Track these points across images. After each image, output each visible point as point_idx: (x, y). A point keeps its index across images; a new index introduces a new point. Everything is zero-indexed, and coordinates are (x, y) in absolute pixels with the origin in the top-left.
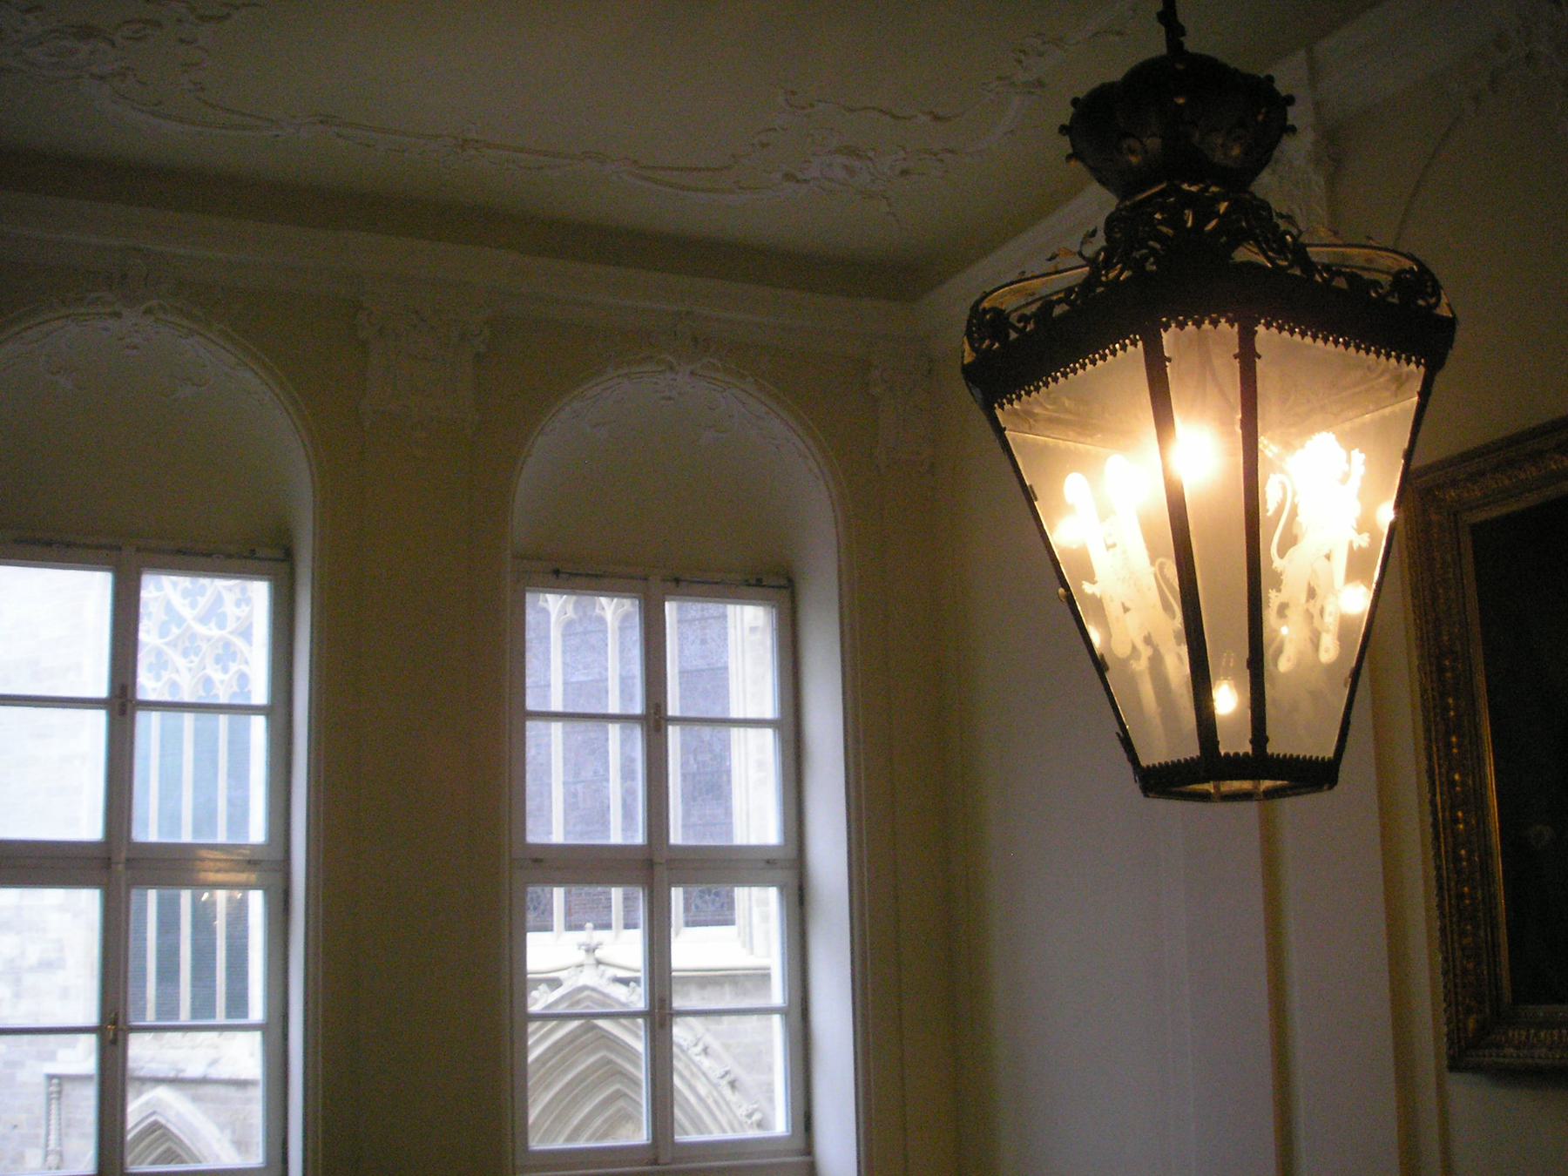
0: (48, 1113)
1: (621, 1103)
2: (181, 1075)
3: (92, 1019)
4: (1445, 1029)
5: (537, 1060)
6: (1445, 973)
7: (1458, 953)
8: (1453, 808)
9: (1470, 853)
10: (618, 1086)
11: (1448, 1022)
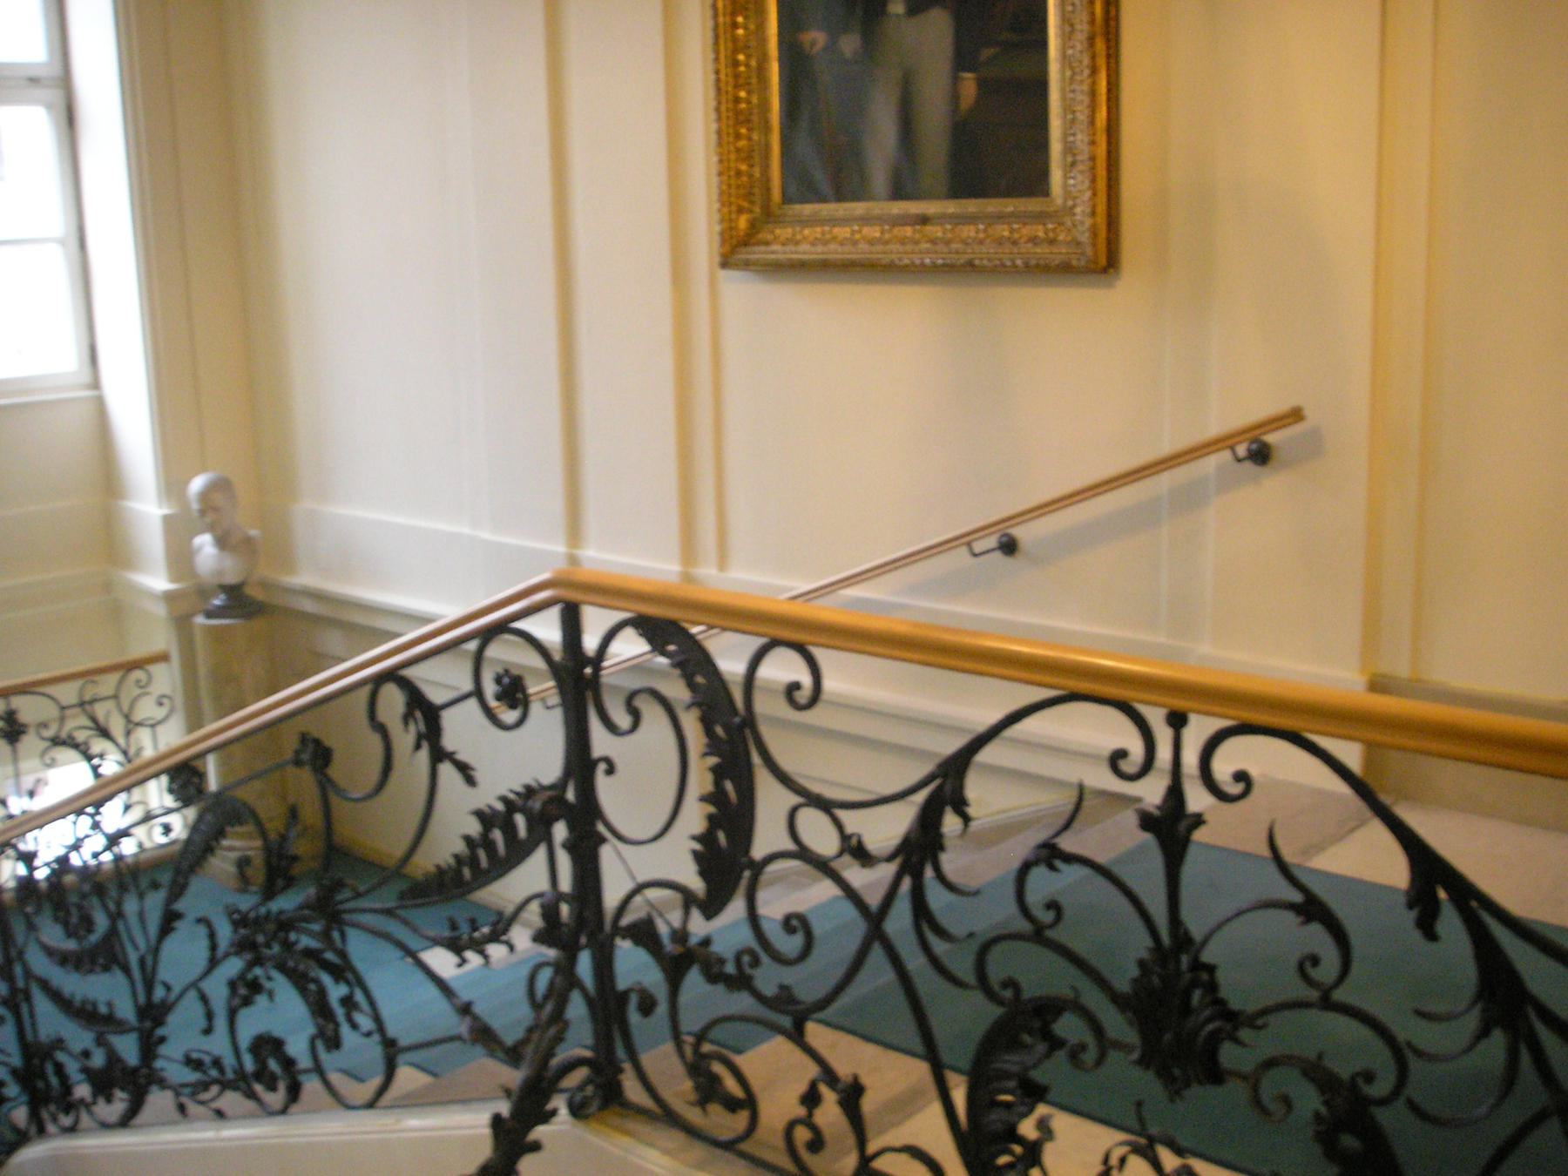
4: (717, 228)
6: (720, 174)
7: (733, 156)
8: (734, 14)
9: (748, 57)
11: (722, 221)
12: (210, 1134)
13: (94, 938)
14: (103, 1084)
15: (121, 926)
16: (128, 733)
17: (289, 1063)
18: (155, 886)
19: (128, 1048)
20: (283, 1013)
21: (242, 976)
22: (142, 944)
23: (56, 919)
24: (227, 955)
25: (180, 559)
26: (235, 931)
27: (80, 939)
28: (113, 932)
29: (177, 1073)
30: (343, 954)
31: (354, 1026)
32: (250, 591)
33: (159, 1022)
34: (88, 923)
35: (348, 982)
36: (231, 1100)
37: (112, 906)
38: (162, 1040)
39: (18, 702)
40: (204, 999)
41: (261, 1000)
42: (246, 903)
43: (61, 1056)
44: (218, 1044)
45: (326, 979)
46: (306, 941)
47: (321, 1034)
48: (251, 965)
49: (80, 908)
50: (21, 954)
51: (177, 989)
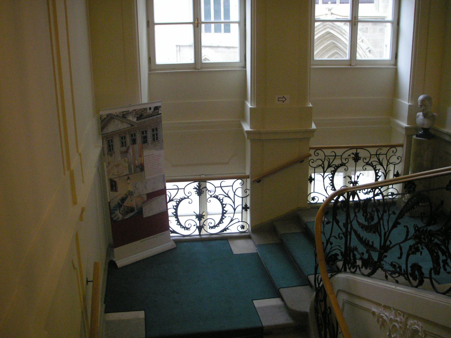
0: (177, 56)
1: (336, 56)
2: (212, 45)
3: (191, 20)
5: (316, 39)
10: (335, 51)
12: (394, 287)
13: (372, 223)
14: (366, 263)
15: (381, 221)
16: (387, 166)
17: (422, 274)
18: (394, 213)
19: (375, 256)
20: (424, 260)
21: (414, 245)
22: (386, 228)
23: (363, 215)
24: (411, 238)
25: (412, 117)
26: (415, 232)
27: (368, 223)
28: (379, 223)
29: (387, 267)
30: (447, 248)
31: (445, 269)
32: (430, 131)
33: (386, 251)
34: (372, 218)
35: (446, 256)
36: (402, 279)
37: (380, 216)
38: (386, 256)
39: (359, 151)
40: (401, 249)
41: (418, 254)
42: (420, 224)
43: (356, 253)
44: (402, 262)
45: (440, 254)
46: (436, 241)
47: (434, 268)
48: (417, 243)
49: (370, 213)
50: (351, 222)
51: (393, 243)
